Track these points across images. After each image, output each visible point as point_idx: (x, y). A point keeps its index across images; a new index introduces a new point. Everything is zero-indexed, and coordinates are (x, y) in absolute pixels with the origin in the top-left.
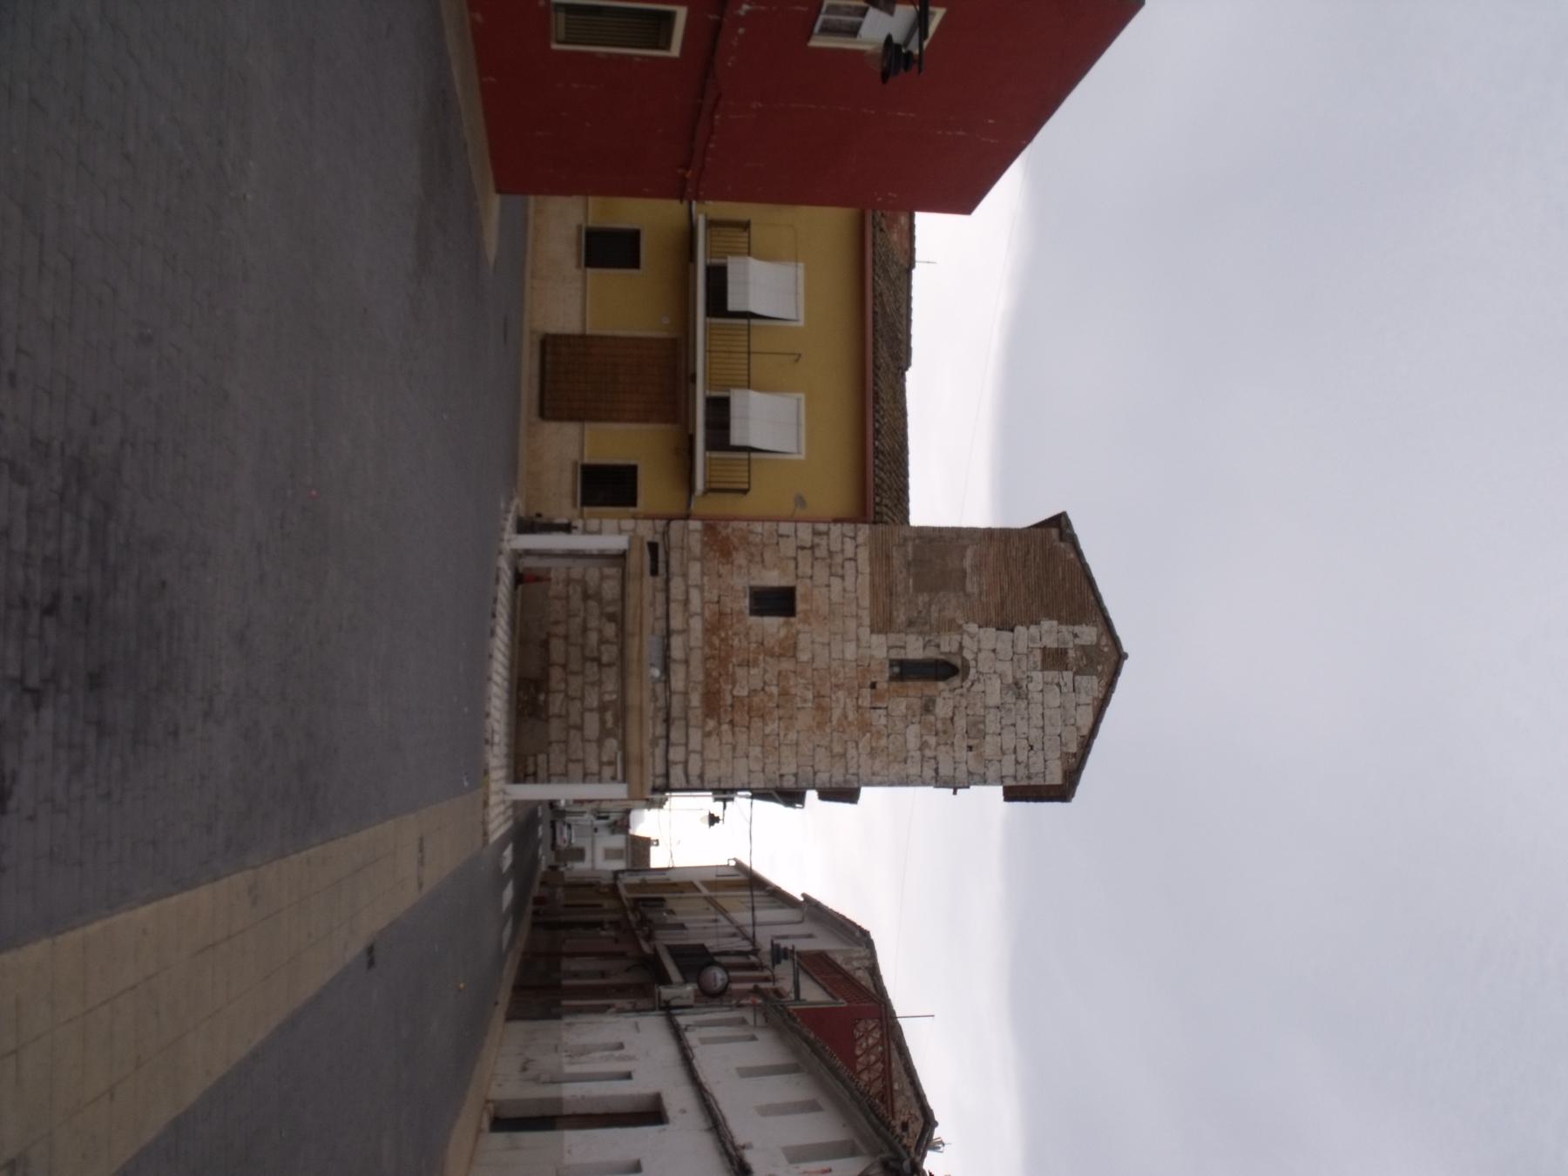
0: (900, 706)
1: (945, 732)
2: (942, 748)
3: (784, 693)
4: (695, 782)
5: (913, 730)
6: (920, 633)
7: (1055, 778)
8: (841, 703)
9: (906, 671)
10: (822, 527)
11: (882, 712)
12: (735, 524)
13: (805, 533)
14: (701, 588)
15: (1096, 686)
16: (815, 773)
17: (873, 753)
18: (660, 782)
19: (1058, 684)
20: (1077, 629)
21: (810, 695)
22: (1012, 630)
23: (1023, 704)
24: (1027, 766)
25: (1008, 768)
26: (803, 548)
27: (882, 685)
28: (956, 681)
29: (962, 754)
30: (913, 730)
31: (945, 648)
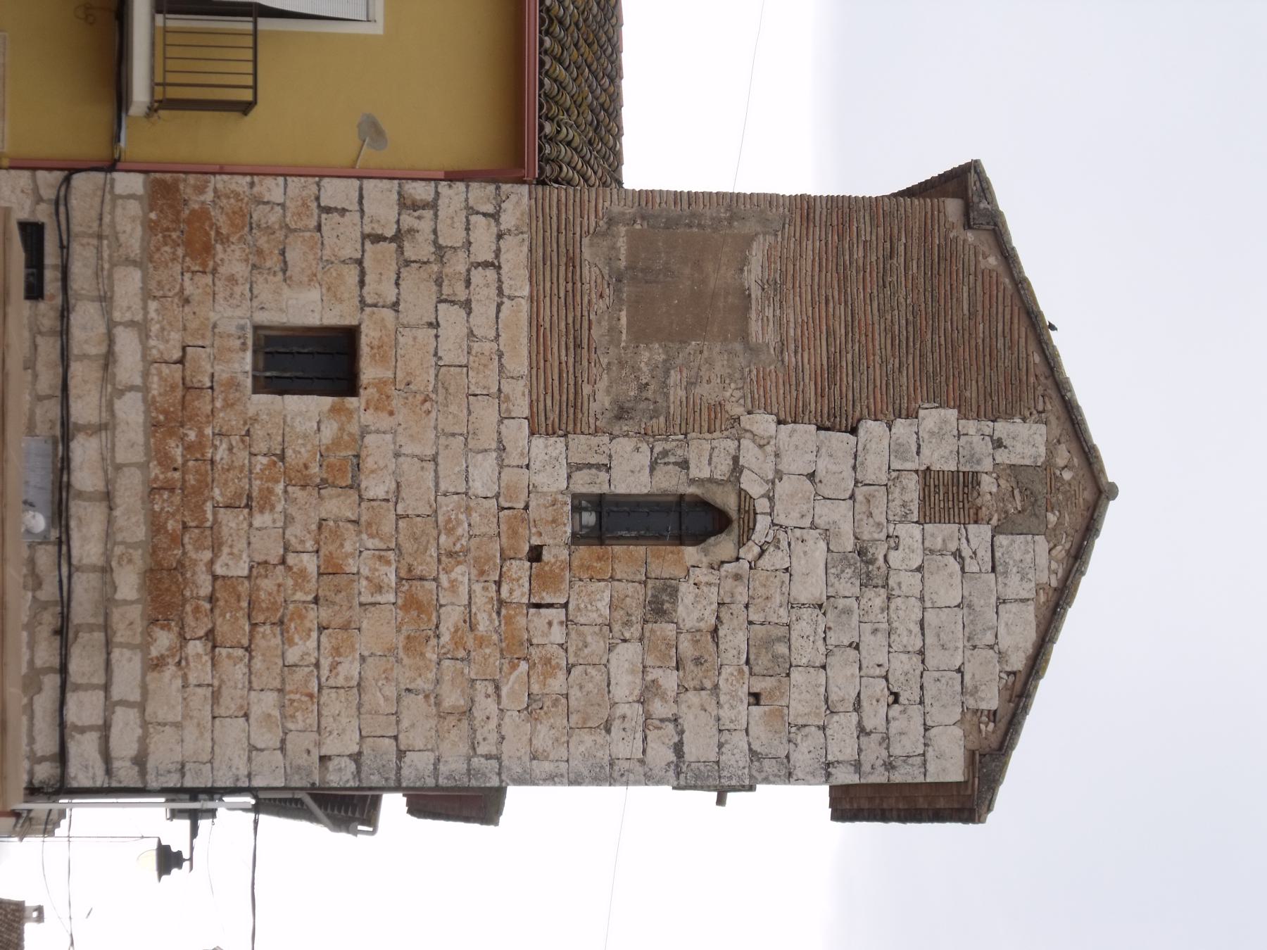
0: (595, 601)
1: (698, 661)
2: (692, 697)
3: (331, 570)
4: (126, 774)
5: (627, 655)
6: (644, 435)
7: (949, 766)
8: (461, 593)
9: (610, 521)
10: (421, 191)
11: (557, 615)
12: (220, 181)
13: (382, 203)
14: (142, 328)
15: (1043, 560)
16: (401, 754)
17: (533, 708)
18: (44, 772)
19: (958, 555)
20: (1002, 428)
21: (389, 575)
22: (853, 431)
23: (876, 599)
24: (886, 739)
25: (843, 745)
26: (377, 239)
27: (555, 554)
28: (724, 546)
29: (737, 711)
30: (627, 655)
31: (700, 470)
